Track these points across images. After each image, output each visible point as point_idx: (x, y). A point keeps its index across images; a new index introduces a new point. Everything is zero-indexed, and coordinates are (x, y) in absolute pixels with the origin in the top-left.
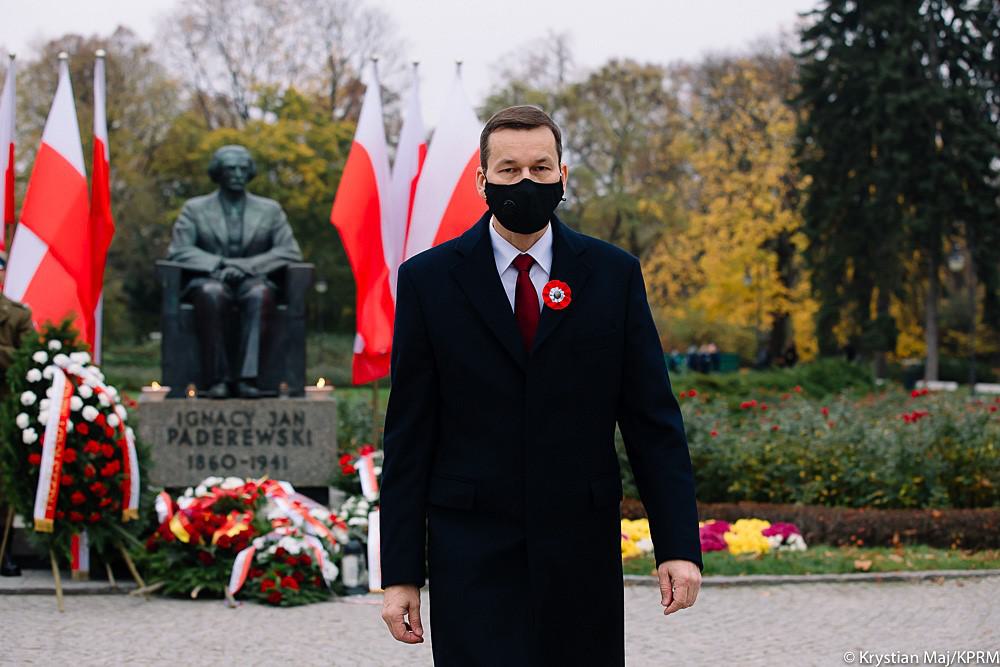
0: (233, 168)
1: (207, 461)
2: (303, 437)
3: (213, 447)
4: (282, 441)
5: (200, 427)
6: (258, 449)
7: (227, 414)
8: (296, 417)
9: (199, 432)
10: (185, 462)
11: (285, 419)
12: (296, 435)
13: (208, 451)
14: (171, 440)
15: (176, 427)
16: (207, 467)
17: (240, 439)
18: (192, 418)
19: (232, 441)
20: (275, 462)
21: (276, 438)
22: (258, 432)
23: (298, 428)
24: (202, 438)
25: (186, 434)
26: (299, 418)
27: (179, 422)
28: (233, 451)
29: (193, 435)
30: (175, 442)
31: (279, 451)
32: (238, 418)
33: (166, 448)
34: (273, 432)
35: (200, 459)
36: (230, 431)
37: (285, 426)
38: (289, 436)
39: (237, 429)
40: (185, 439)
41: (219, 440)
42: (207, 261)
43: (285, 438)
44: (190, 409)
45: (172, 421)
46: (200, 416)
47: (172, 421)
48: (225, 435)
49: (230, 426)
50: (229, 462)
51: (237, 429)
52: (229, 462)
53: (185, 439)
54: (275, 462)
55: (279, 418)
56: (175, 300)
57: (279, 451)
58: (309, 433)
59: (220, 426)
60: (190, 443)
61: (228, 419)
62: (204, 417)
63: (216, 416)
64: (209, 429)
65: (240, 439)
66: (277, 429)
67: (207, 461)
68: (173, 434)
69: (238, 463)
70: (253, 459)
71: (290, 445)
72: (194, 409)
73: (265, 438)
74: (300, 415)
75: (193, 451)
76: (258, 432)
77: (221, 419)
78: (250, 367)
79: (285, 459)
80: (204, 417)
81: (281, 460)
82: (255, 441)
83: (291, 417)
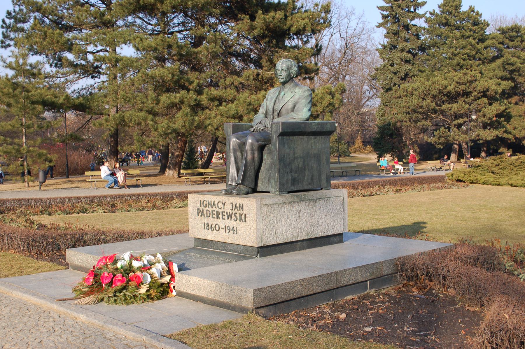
1: (210, 226)
2: (243, 217)
5: (207, 208)
9: (207, 210)
10: (203, 226)
12: (241, 215)
13: (212, 221)
14: (198, 213)
16: (210, 229)
17: (220, 216)
19: (218, 217)
20: (233, 229)
23: (241, 212)
24: (208, 215)
26: (242, 208)
27: (201, 206)
34: (232, 213)
35: (208, 224)
38: (238, 216)
48: (215, 213)
52: (217, 229)
58: (245, 215)
59: (214, 209)
64: (211, 210)
65: (220, 216)
66: (234, 212)
67: (210, 226)
69: (220, 229)
70: (225, 226)
73: (229, 216)
75: (206, 220)
76: (227, 212)
81: (235, 228)
82: (226, 217)
83: (238, 207)
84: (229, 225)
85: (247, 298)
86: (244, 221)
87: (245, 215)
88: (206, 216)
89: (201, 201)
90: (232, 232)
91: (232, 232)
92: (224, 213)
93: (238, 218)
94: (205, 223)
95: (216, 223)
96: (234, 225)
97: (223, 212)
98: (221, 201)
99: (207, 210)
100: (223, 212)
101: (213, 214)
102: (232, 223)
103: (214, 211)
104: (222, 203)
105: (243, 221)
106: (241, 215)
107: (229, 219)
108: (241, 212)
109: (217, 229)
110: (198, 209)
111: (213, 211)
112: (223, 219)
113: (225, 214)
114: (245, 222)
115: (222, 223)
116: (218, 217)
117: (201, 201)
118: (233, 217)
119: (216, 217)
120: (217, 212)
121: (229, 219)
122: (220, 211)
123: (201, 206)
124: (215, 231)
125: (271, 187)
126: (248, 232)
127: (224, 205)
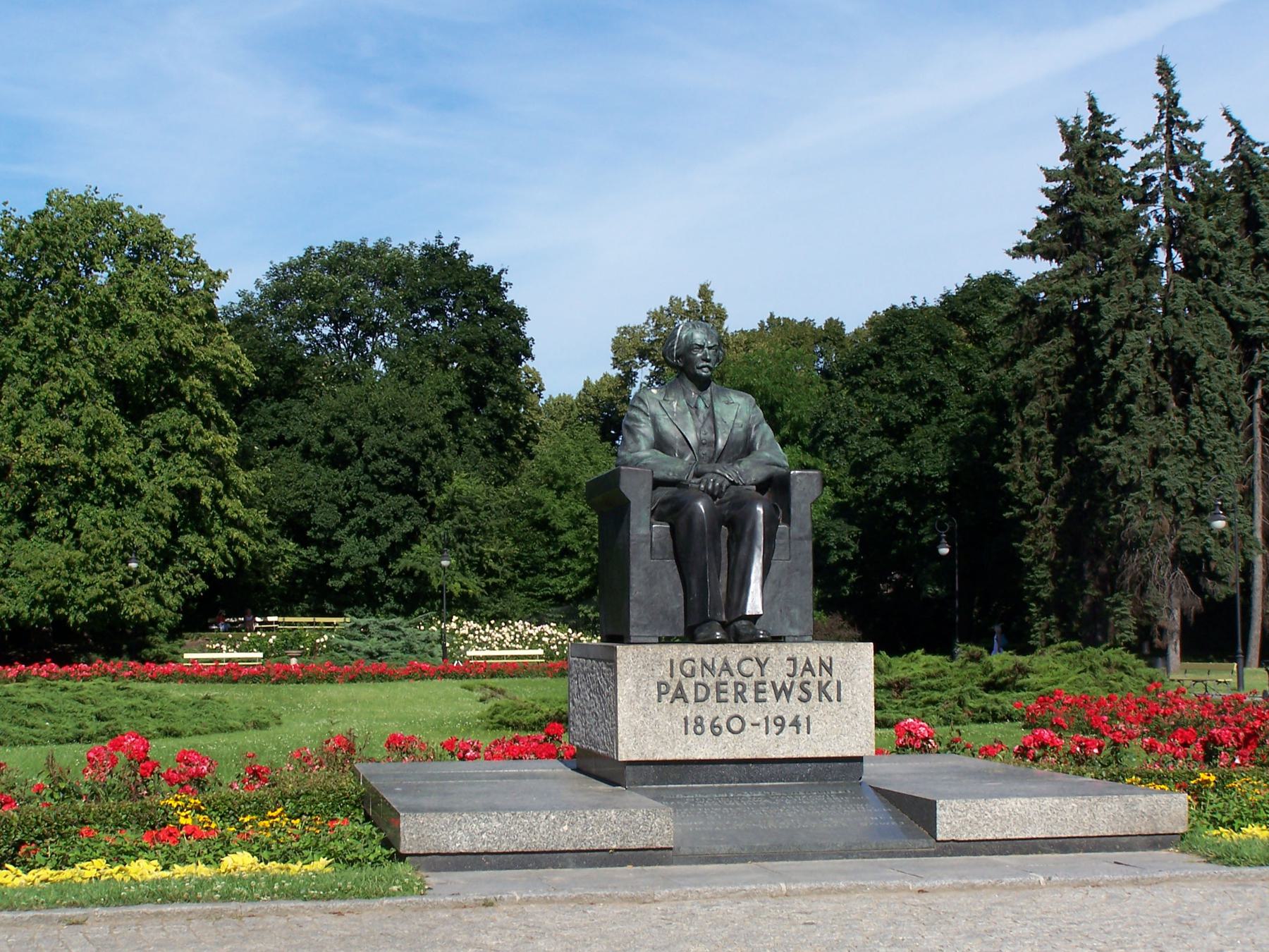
0: (702, 347)
1: (707, 724)
3: (715, 704)
4: (805, 696)
5: (699, 679)
6: (774, 707)
7: (733, 664)
8: (822, 663)
9: (697, 684)
11: (808, 668)
12: (822, 689)
13: (709, 710)
14: (660, 694)
15: (668, 679)
16: (708, 731)
17: (750, 694)
18: (688, 670)
19: (740, 696)
21: (796, 692)
22: (773, 683)
24: (701, 695)
25: (680, 687)
27: (672, 676)
28: (740, 709)
29: (690, 692)
30: (666, 699)
31: (802, 710)
32: (746, 667)
33: (654, 706)
34: (792, 683)
35: (699, 722)
36: (736, 684)
37: (808, 676)
39: (746, 681)
40: (680, 695)
41: (723, 696)
42: (674, 467)
43: (808, 693)
44: (684, 656)
45: (662, 672)
46: (699, 664)
47: (662, 672)
49: (738, 677)
50: (736, 725)
51: (746, 681)
53: (680, 695)
54: (796, 723)
55: (801, 666)
56: (646, 515)
57: (802, 710)
58: (839, 683)
59: (725, 676)
60: (686, 701)
61: (734, 669)
62: (704, 664)
63: (718, 665)
64: (711, 681)
65: (750, 694)
66: (798, 681)
67: (707, 724)
68: (663, 688)
69: (748, 726)
70: (766, 719)
71: (814, 701)
72: (691, 655)
73: (782, 692)
74: (827, 663)
75: (690, 711)
76: (773, 683)
77: (726, 667)
78: (754, 603)
79: (808, 718)
80: (704, 664)
82: (770, 695)
83: (816, 665)
84: (781, 714)
85: (1174, 814)
86: (834, 696)
87: (839, 683)
88: (691, 698)
89: (672, 661)
90: (789, 731)
91: (789, 731)
92: (761, 687)
93: (815, 693)
94: (686, 719)
95: (729, 713)
96: (800, 713)
97: (757, 684)
98: (753, 656)
99: (697, 684)
100: (757, 684)
101: (719, 691)
102: (792, 708)
103: (726, 683)
104: (758, 660)
105: (830, 700)
106: (822, 689)
107: (783, 697)
108: (825, 677)
109: (736, 725)
110: (660, 684)
111: (718, 684)
112: (757, 701)
113: (768, 687)
114: (839, 700)
115: (752, 712)
116: (740, 696)
117: (672, 661)
118: (796, 692)
119: (731, 698)
120: (736, 684)
121: (783, 697)
122: (749, 682)
123: (672, 676)
124: (726, 735)
125: (788, 624)
126: (848, 723)
127: (762, 666)
